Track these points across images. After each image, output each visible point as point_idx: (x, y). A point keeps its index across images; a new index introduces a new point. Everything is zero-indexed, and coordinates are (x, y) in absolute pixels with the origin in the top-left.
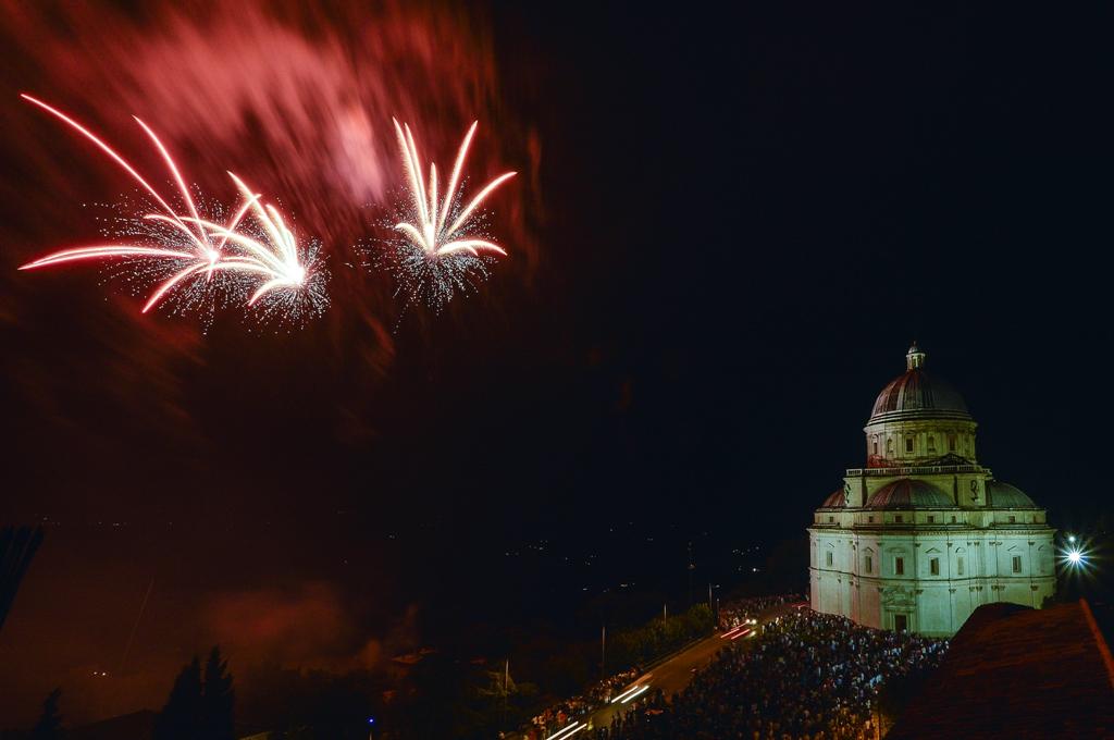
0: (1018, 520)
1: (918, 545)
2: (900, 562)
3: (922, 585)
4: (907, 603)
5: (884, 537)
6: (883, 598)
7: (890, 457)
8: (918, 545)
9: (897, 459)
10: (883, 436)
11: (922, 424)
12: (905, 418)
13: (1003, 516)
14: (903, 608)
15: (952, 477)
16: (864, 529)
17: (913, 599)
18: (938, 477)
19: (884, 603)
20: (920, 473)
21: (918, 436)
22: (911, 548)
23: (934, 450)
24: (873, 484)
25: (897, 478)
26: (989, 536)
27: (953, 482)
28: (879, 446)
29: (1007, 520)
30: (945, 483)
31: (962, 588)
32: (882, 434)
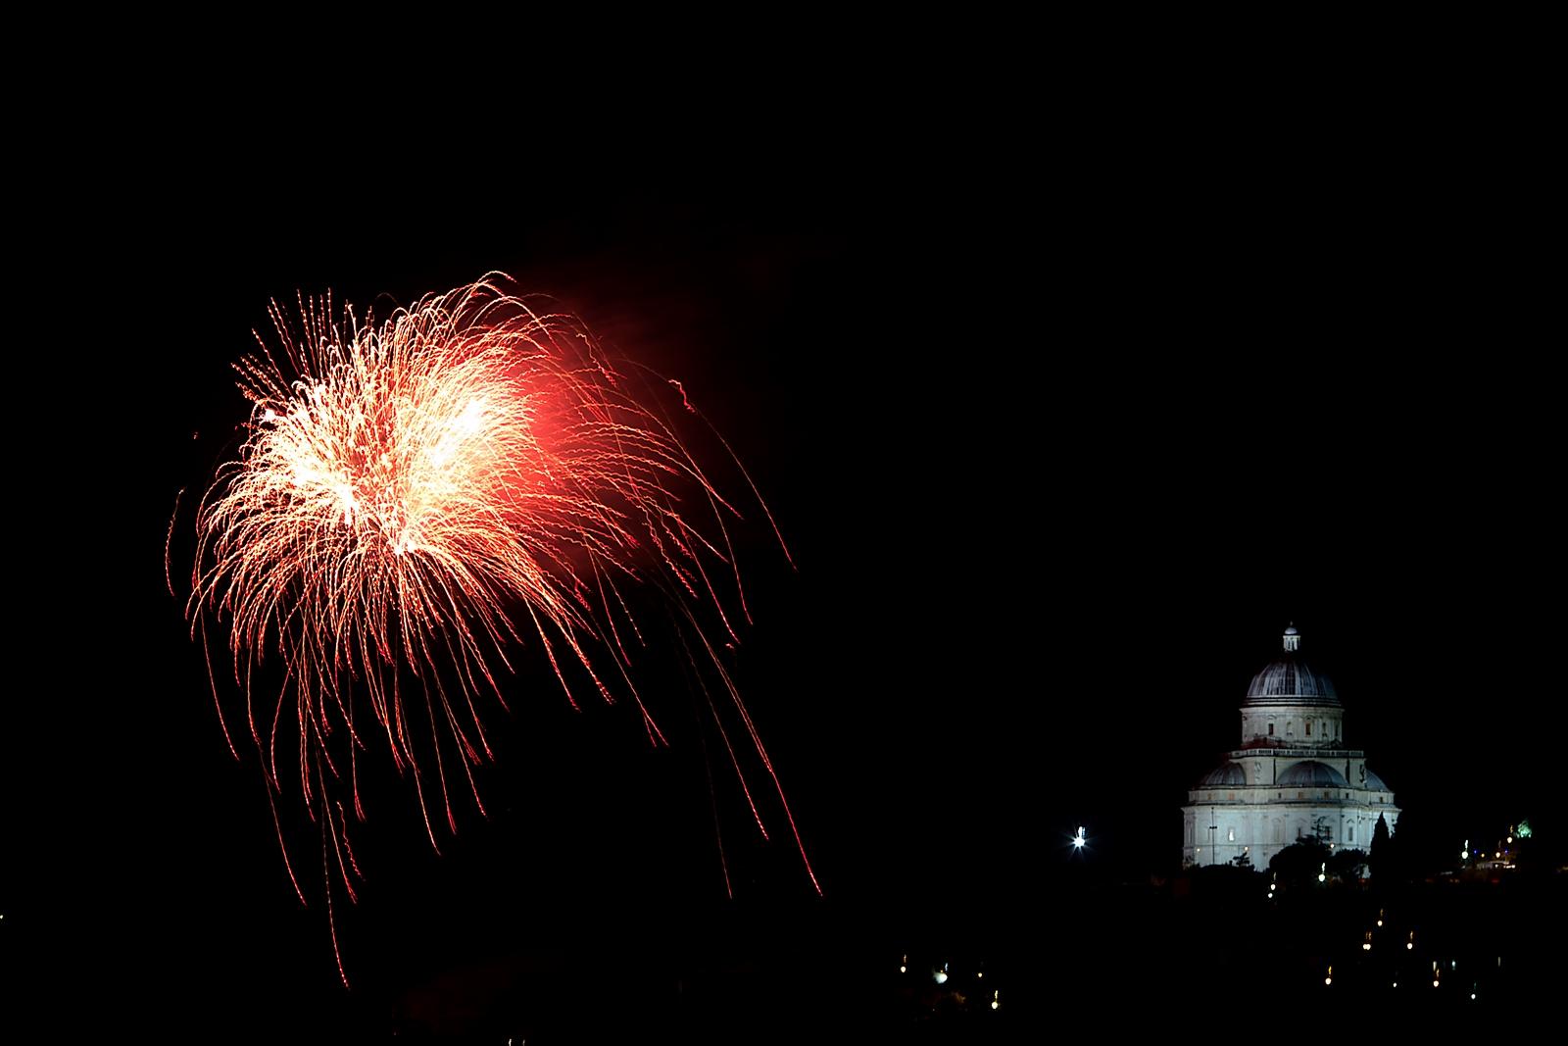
0: (1385, 800)
5: (1318, 809)
7: (1289, 739)
8: (1343, 816)
9: (1298, 741)
10: (1282, 719)
11: (1320, 710)
12: (1306, 703)
13: (1375, 796)
15: (1346, 760)
16: (1290, 803)
18: (1336, 760)
20: (1319, 755)
22: (1338, 819)
24: (1283, 764)
25: (1301, 760)
27: (1346, 765)
29: (1378, 800)
30: (1339, 765)
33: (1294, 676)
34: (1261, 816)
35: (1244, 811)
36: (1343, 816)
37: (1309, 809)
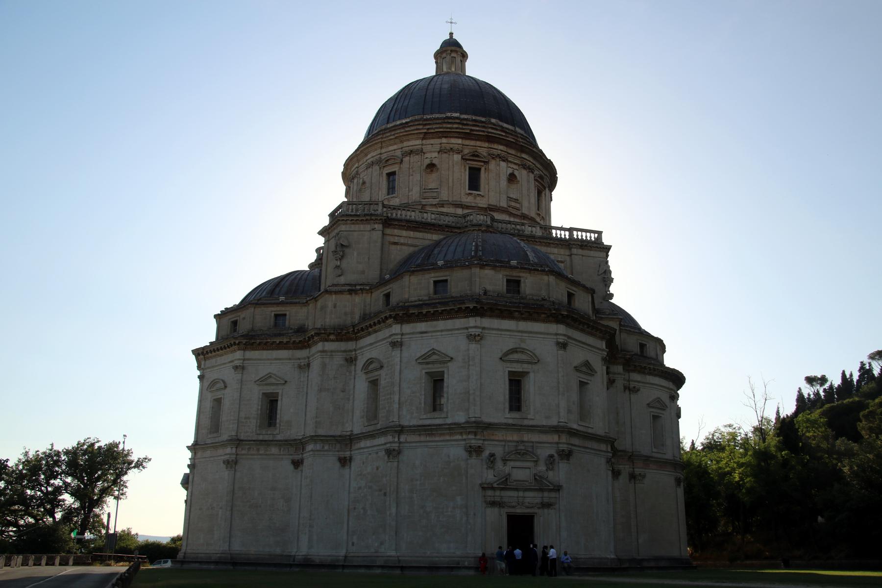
5: (486, 322)
10: (415, 158)
19: (485, 487)
21: (492, 165)
28: (400, 180)
29: (637, 350)
34: (338, 360)
35: (303, 353)
36: (563, 346)
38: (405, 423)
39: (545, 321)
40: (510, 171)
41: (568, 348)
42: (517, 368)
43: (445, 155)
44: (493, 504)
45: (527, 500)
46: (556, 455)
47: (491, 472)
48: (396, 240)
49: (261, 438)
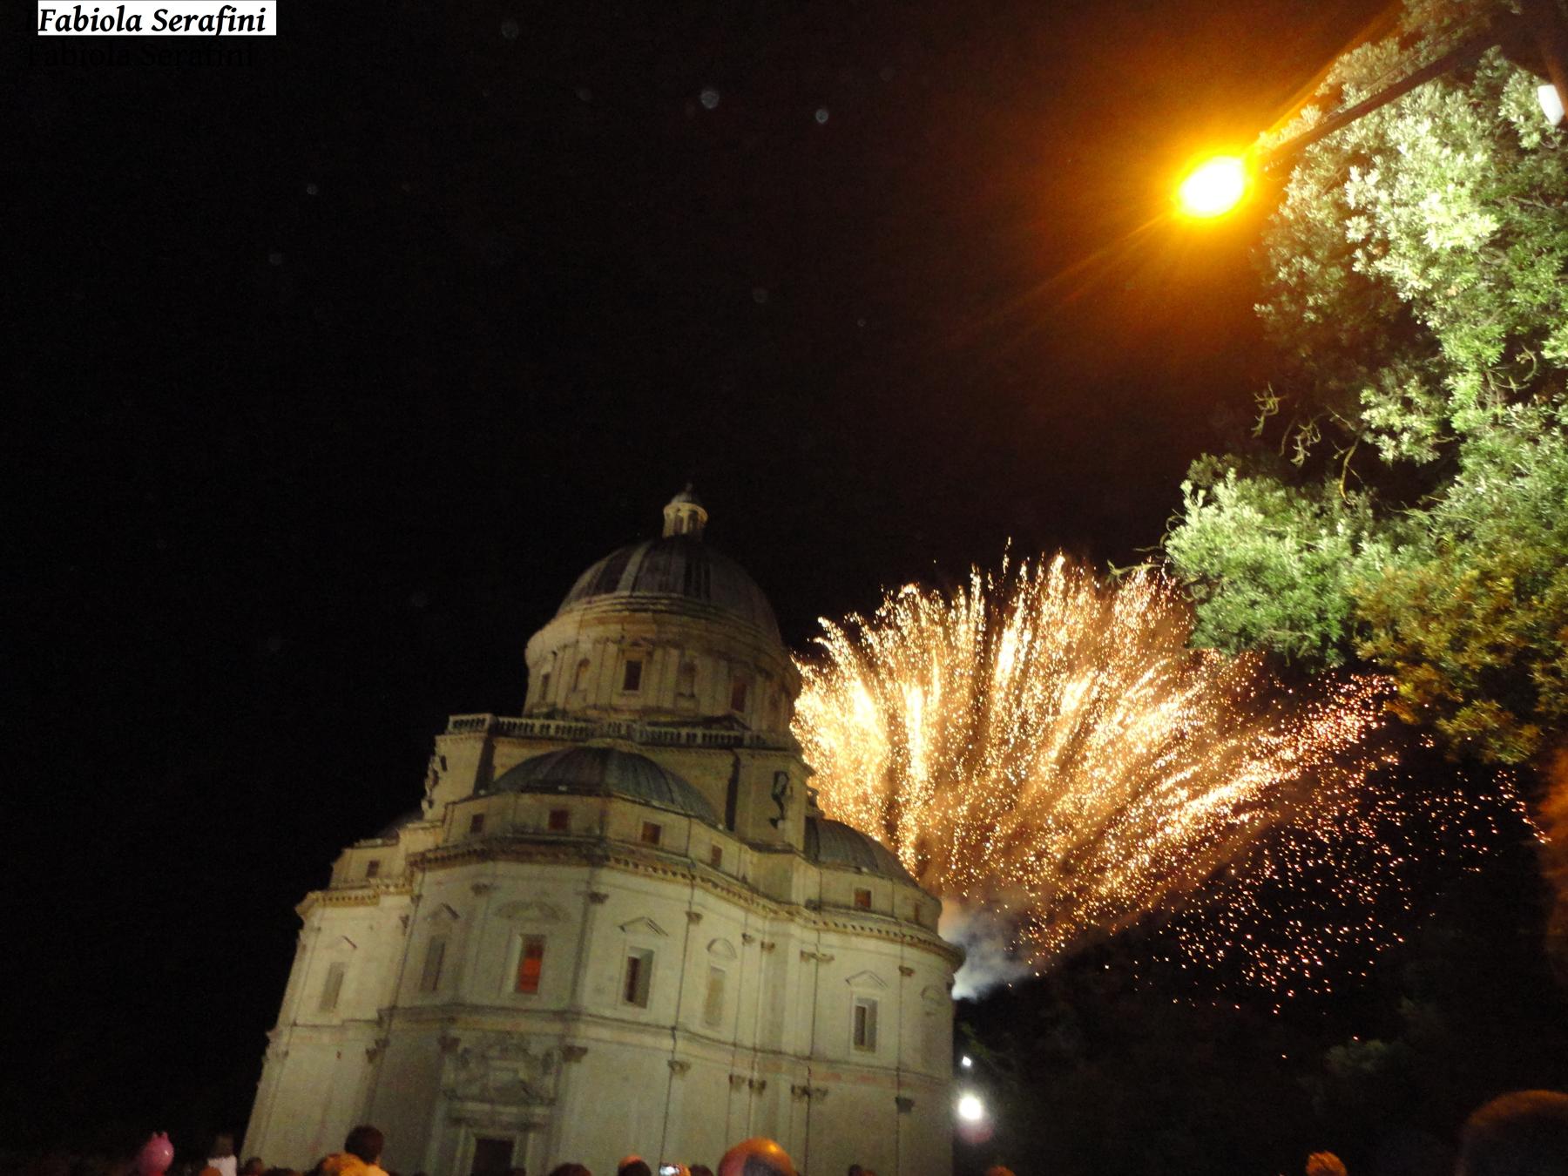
0: (878, 902)
1: (597, 898)
2: (534, 951)
3: (586, 1034)
4: (525, 1093)
6: (450, 1075)
8: (597, 898)
9: (595, 707)
10: (569, 652)
14: (509, 1113)
17: (549, 1081)
19: (451, 1095)
21: (658, 654)
22: (574, 906)
23: (692, 696)
24: (509, 755)
26: (800, 934)
28: (553, 681)
31: (709, 1069)
32: (572, 644)
33: (628, 558)
34: (395, 920)
37: (473, 868)
38: (400, 1004)
39: (578, 865)
40: (687, 660)
41: (608, 902)
42: (531, 929)
43: (600, 647)
44: (457, 1121)
45: (505, 1119)
46: (556, 1056)
47: (463, 1075)
48: (504, 760)
49: (318, 1022)
